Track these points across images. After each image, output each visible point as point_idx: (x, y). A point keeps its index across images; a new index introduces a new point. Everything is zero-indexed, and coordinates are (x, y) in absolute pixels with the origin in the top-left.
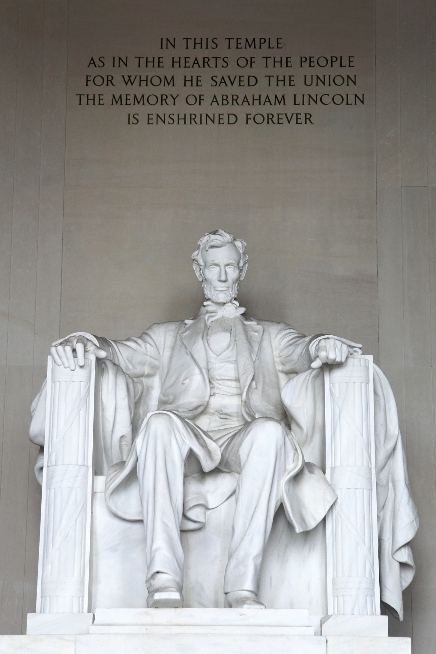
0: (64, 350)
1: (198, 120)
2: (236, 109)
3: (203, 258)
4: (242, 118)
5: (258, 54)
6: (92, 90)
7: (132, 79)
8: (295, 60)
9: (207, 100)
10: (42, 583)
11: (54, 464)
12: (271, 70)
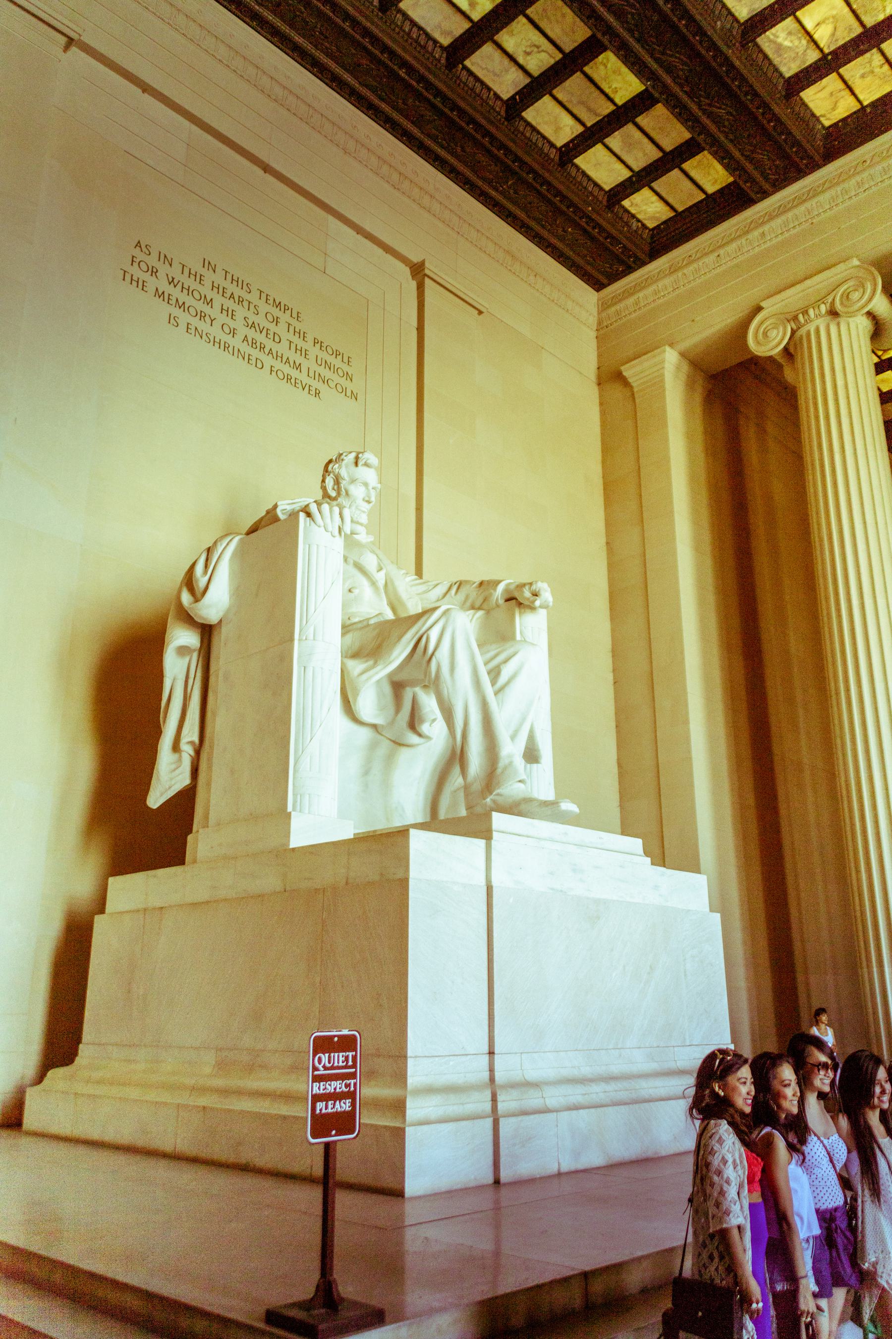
0: (331, 511)
1: (231, 349)
2: (262, 356)
3: (348, 473)
4: (267, 368)
5: (285, 317)
6: (135, 271)
7: (176, 281)
8: (310, 338)
9: (240, 337)
10: (294, 778)
11: (311, 637)
12: (290, 336)
